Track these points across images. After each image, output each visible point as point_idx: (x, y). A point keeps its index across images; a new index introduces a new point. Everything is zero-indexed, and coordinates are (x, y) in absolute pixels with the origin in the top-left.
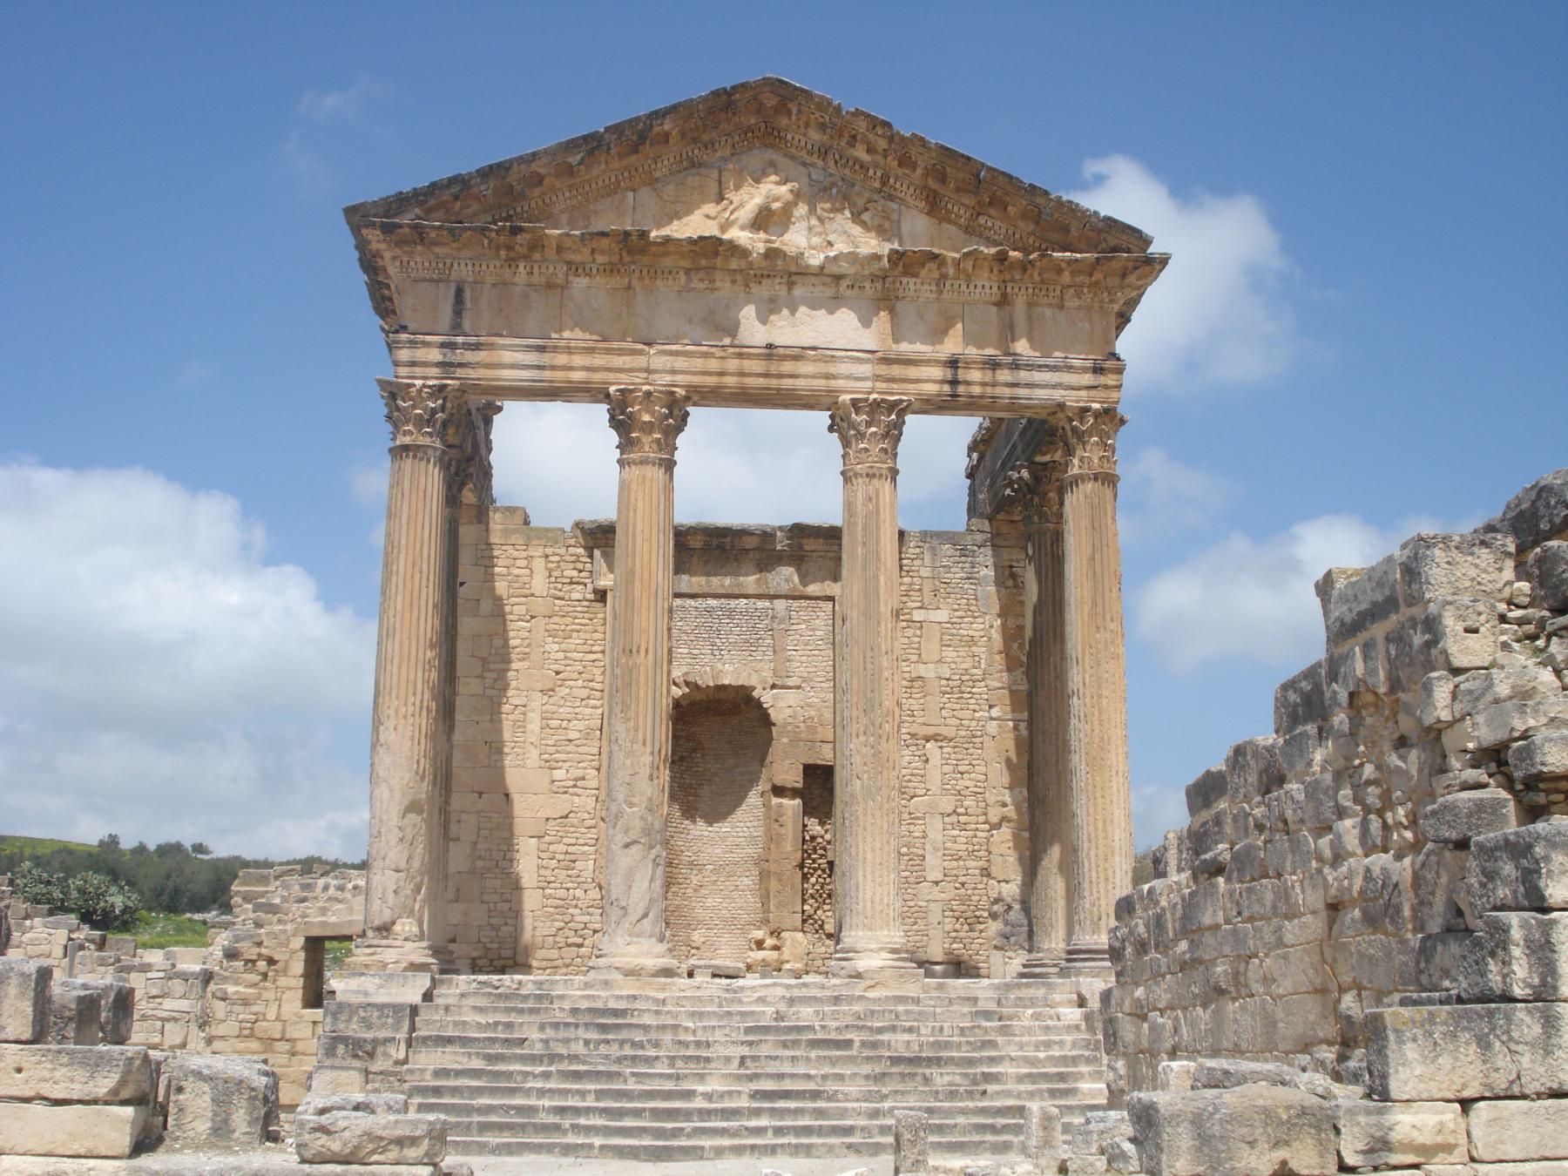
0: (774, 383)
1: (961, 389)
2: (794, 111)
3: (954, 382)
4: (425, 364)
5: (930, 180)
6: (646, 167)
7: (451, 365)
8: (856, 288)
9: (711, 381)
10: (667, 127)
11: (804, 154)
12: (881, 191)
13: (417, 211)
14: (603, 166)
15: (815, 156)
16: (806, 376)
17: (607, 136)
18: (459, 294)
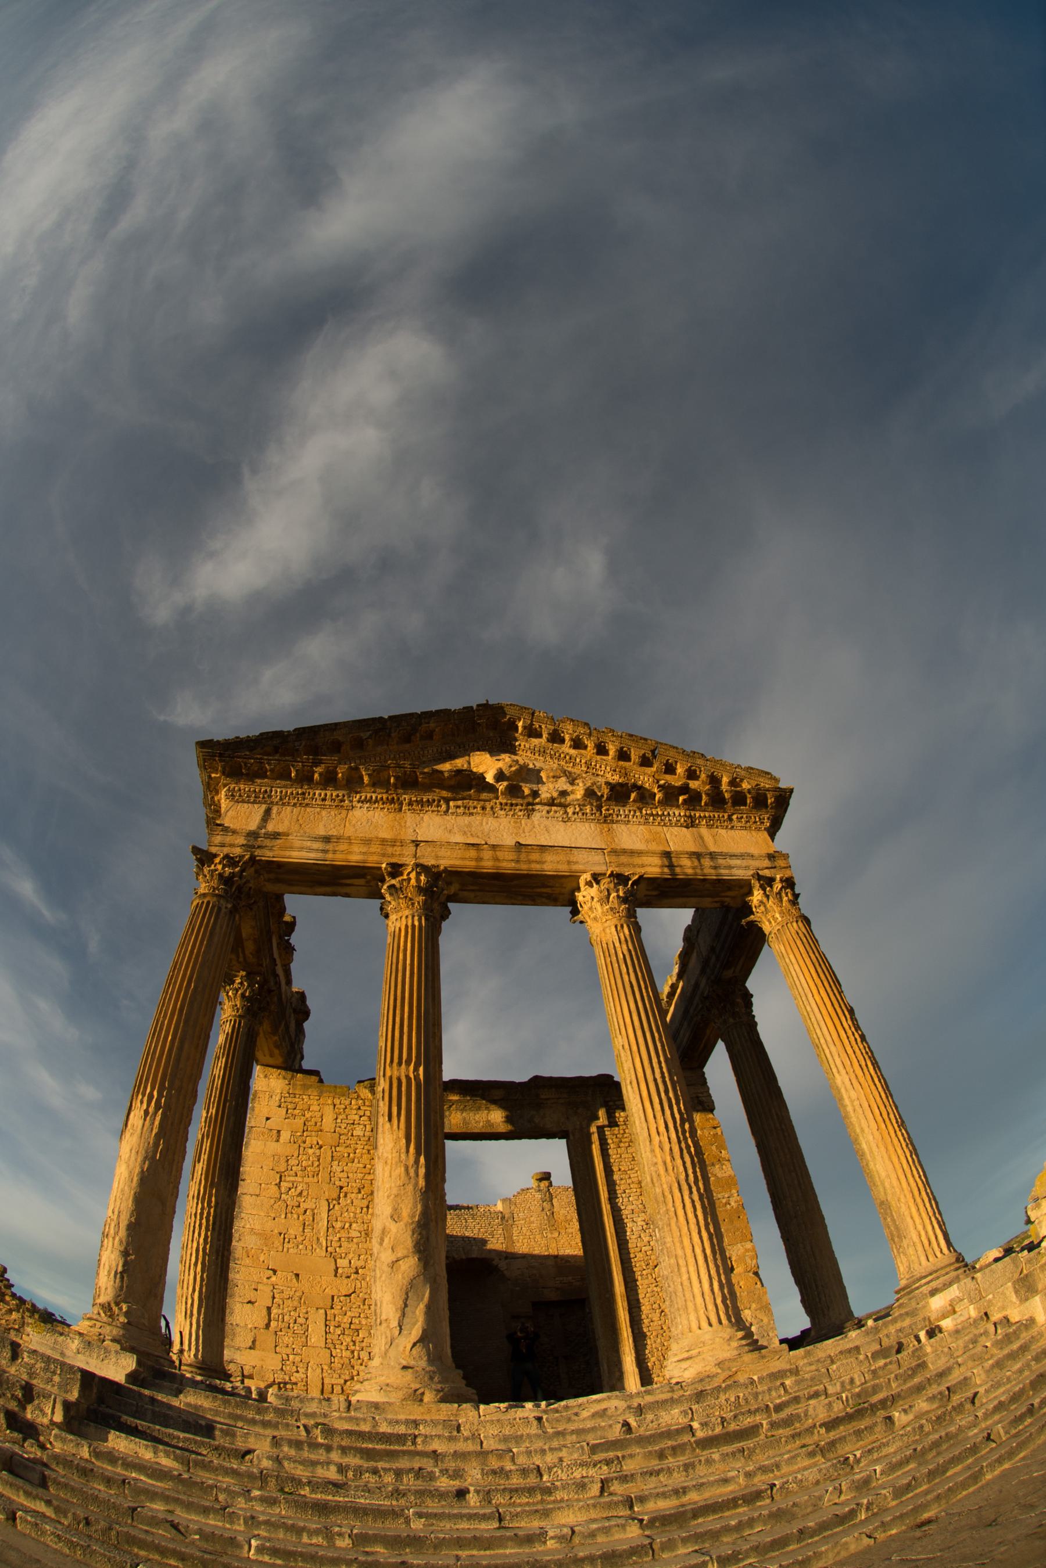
0: (524, 866)
1: (678, 870)
2: (520, 724)
3: (671, 866)
4: (232, 845)
5: (621, 763)
6: (416, 752)
7: (254, 847)
8: (580, 814)
9: (473, 863)
10: (432, 725)
11: (529, 754)
12: (587, 772)
13: (248, 753)
14: (385, 747)
15: (537, 754)
16: (551, 865)
17: (388, 723)
18: (268, 812)
